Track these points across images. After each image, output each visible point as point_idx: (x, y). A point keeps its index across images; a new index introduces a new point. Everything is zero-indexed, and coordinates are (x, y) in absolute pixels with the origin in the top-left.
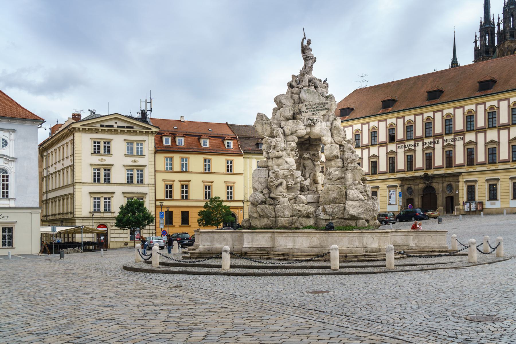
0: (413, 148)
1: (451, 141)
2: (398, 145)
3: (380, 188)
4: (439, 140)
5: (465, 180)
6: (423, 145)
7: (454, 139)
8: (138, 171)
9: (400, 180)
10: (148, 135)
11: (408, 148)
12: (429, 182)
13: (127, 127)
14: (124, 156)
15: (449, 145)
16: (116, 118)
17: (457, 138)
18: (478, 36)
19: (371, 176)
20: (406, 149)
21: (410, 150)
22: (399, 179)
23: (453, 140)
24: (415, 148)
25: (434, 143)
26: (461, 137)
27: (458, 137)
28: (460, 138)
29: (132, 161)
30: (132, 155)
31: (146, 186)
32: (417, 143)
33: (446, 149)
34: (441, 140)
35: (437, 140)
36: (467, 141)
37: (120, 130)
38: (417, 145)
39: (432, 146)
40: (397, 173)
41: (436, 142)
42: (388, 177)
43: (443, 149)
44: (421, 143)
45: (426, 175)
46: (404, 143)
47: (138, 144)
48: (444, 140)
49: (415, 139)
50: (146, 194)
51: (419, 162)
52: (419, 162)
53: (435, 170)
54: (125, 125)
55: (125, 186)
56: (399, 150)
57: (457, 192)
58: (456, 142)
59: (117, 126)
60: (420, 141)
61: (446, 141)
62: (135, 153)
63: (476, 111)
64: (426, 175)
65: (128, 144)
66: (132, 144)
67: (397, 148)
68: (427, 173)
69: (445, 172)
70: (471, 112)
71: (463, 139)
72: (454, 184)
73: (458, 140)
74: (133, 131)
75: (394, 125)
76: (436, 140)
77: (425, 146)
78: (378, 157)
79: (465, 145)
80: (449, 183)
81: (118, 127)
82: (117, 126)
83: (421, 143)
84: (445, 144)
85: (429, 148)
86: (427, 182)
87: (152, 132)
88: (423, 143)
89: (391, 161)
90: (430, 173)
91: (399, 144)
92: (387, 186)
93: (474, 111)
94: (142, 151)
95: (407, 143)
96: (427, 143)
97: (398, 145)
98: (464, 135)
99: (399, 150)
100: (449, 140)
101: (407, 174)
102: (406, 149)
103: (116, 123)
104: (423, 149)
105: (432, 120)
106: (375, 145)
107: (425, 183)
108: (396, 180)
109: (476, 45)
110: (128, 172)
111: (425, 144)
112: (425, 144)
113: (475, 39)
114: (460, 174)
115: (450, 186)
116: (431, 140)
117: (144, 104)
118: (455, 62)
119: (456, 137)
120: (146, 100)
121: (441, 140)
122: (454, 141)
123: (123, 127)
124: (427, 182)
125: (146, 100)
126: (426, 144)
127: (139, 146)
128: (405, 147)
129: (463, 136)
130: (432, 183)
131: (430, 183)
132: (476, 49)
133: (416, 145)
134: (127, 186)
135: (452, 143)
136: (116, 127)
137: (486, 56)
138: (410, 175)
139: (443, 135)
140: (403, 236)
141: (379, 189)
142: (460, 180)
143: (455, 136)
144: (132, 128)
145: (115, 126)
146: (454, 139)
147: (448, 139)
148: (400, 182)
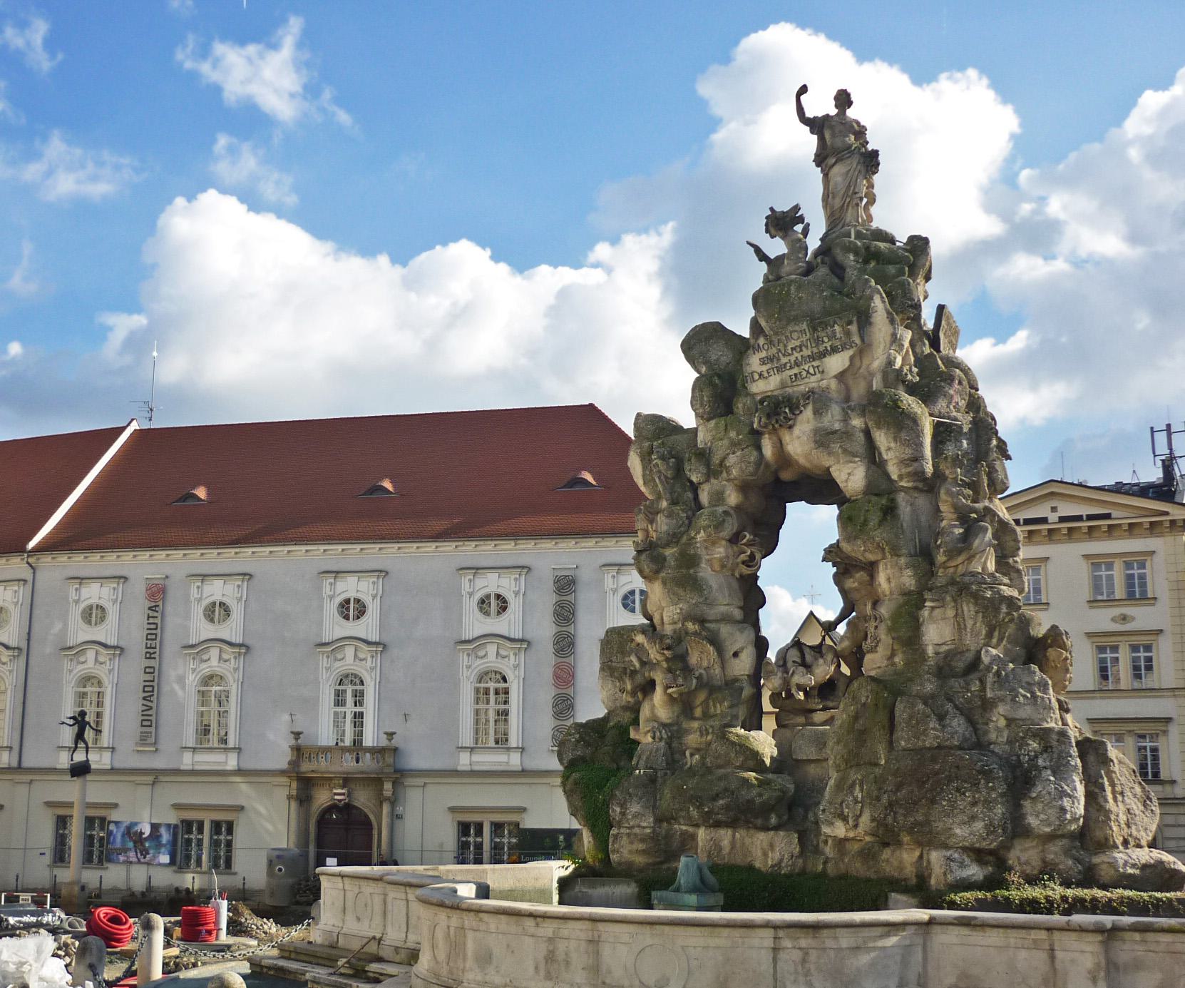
8: (1135, 648)
10: (1161, 535)
13: (1090, 517)
14: (1087, 605)
16: (1052, 494)
29: (1113, 620)
30: (1111, 602)
31: (1168, 697)
37: (1072, 528)
47: (1128, 565)
50: (1168, 720)
54: (1084, 510)
55: (1093, 698)
59: (1060, 517)
62: (1120, 592)
65: (1096, 566)
66: (1110, 566)
74: (1109, 526)
81: (1063, 519)
82: (1060, 517)
87: (1173, 522)
94: (1143, 585)
103: (1054, 509)
110: (1134, 655)
117: (1161, 438)
120: (1169, 426)
123: (1078, 518)
125: (1169, 426)
127: (1104, 573)
134: (1101, 698)
136: (1057, 520)
140: (1023, 954)
144: (1107, 516)
145: (1053, 517)
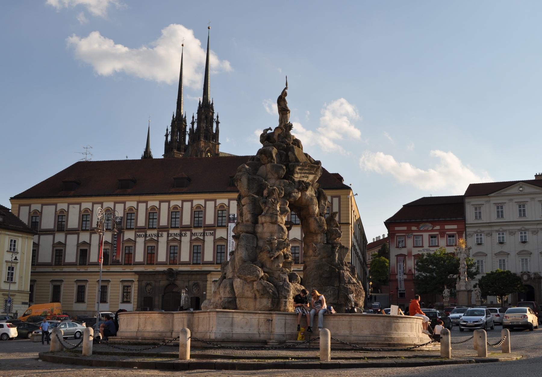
0: (156, 238)
1: (200, 235)
2: (137, 233)
3: (89, 283)
4: (187, 232)
5: (214, 279)
6: (168, 236)
7: (204, 233)
9: (138, 274)
11: (149, 238)
12: (173, 279)
15: (197, 239)
17: (207, 233)
18: (170, 130)
19: (78, 266)
20: (147, 239)
21: (152, 240)
22: (136, 273)
23: (202, 234)
24: (158, 239)
25: (181, 235)
26: (212, 232)
27: (208, 232)
28: (210, 233)
32: (160, 233)
33: (195, 244)
34: (188, 233)
35: (184, 232)
36: (218, 236)
38: (161, 235)
39: (178, 238)
40: (134, 266)
41: (184, 235)
42: (123, 270)
43: (191, 243)
44: (165, 234)
45: (170, 270)
46: (146, 232)
48: (193, 233)
49: (158, 228)
51: (162, 256)
52: (162, 256)
53: (180, 265)
56: (138, 239)
57: (204, 293)
58: (206, 237)
60: (165, 231)
61: (194, 234)
63: (205, 207)
64: (170, 270)
67: (136, 236)
68: (172, 269)
69: (191, 269)
70: (224, 207)
71: (214, 234)
72: (201, 283)
73: (208, 235)
75: (134, 210)
76: (183, 232)
77: (170, 238)
78: (89, 245)
79: (215, 241)
80: (196, 282)
83: (165, 234)
84: (193, 238)
85: (174, 240)
86: (170, 279)
88: (168, 234)
89: (127, 251)
90: (175, 268)
91: (139, 232)
92: (121, 280)
93: (226, 206)
95: (149, 232)
96: (173, 235)
97: (137, 233)
98: (215, 230)
99: (138, 239)
100: (198, 234)
101: (146, 268)
102: (147, 239)
104: (168, 240)
105: (180, 210)
106: (86, 230)
107: (168, 280)
108: (133, 273)
109: (167, 139)
111: (170, 235)
112: (170, 235)
113: (166, 132)
114: (209, 272)
115: (196, 285)
116: (177, 231)
118: (147, 153)
119: (206, 232)
121: (188, 233)
122: (204, 236)
124: (170, 279)
126: (171, 235)
128: (146, 236)
129: (213, 231)
130: (177, 280)
131: (174, 280)
132: (166, 142)
133: (160, 235)
135: (202, 238)
137: (177, 152)
138: (150, 269)
139: (191, 227)
141: (110, 283)
142: (208, 279)
143: (204, 230)
146: (204, 233)
147: (197, 233)
148: (137, 277)
